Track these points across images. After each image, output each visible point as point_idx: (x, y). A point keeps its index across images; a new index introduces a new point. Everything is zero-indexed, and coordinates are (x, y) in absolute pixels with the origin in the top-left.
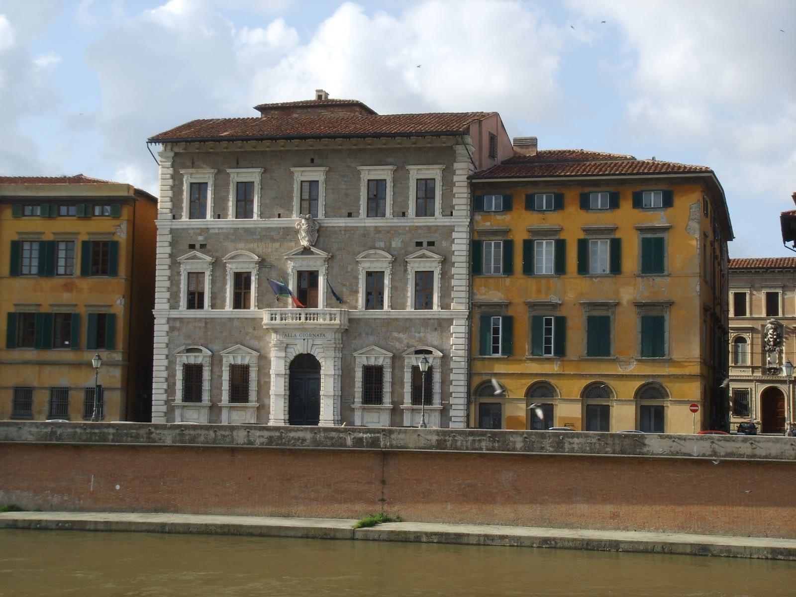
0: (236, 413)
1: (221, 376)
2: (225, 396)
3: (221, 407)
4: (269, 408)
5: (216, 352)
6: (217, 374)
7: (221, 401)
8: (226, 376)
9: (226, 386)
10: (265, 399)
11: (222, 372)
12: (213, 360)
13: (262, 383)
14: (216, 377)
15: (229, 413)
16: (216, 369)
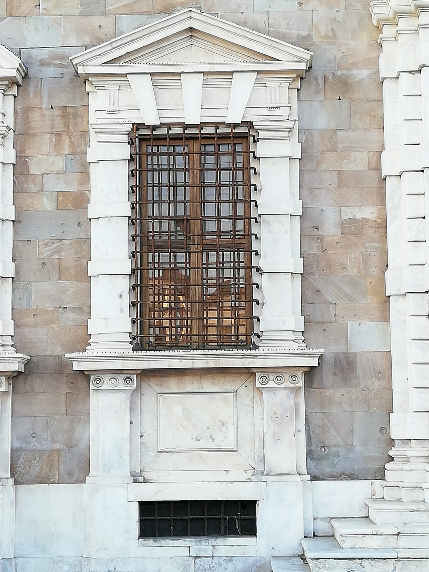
0: (177, 410)
1: (81, 201)
2: (111, 312)
3: (84, 375)
4: (385, 373)
5: (43, 63)
6: (56, 185)
7: (83, 341)
8: (110, 191)
9: (111, 249)
10: (352, 325)
11: (85, 171)
12: (27, 110)
13: (330, 229)
14: (47, 204)
15: (132, 409)
16: (46, 161)
